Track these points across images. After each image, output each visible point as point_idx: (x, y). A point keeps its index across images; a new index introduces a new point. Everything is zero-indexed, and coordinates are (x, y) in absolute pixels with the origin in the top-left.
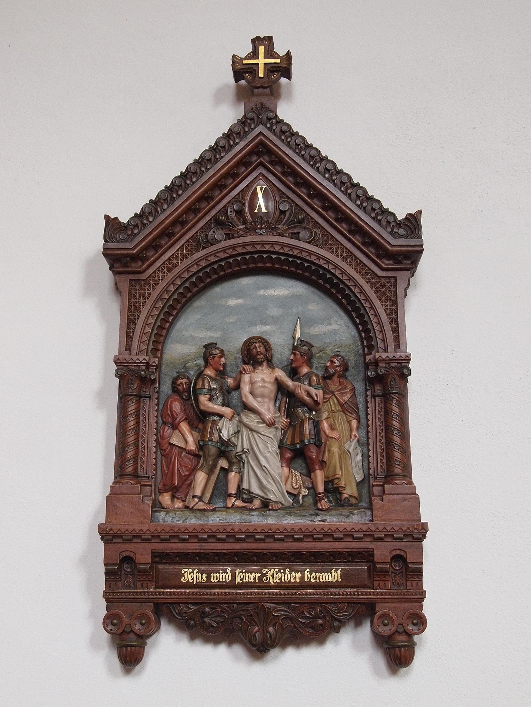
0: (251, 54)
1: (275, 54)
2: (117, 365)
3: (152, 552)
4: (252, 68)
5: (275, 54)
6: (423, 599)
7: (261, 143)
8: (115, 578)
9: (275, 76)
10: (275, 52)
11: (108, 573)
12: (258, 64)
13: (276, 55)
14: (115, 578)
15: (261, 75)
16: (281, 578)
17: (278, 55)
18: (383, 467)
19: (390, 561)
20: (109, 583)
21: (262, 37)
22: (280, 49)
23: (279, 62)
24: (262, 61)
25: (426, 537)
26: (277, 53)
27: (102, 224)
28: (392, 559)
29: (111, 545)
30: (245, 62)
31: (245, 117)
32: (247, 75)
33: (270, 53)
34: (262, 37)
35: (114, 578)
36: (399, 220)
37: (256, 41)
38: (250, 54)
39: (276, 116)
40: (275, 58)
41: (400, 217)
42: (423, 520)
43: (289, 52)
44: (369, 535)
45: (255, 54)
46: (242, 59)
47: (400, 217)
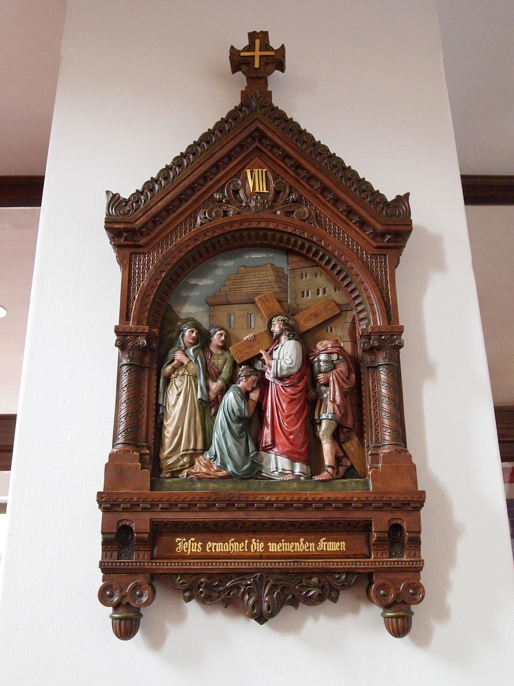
0: (248, 47)
1: (269, 48)
2: (117, 335)
3: (151, 521)
4: (248, 60)
5: (269, 48)
6: (421, 569)
7: (258, 129)
8: (112, 547)
9: (269, 67)
10: (270, 46)
11: (106, 543)
12: (254, 56)
13: (271, 49)
14: (112, 547)
15: (257, 66)
16: (282, 547)
17: (273, 49)
18: (378, 437)
19: (388, 530)
20: (105, 552)
21: (258, 32)
22: (275, 44)
23: (274, 54)
24: (257, 54)
25: (423, 506)
26: (271, 47)
27: (104, 201)
28: (390, 528)
29: (108, 514)
30: (242, 54)
31: (241, 103)
32: (243, 66)
33: (266, 46)
34: (258, 32)
35: (110, 548)
36: (389, 200)
37: (252, 36)
38: (246, 47)
39: (271, 104)
40: (271, 51)
41: (390, 198)
42: (420, 489)
43: (283, 45)
44: (366, 505)
45: (250, 47)
46: (239, 52)
47: (390, 198)
